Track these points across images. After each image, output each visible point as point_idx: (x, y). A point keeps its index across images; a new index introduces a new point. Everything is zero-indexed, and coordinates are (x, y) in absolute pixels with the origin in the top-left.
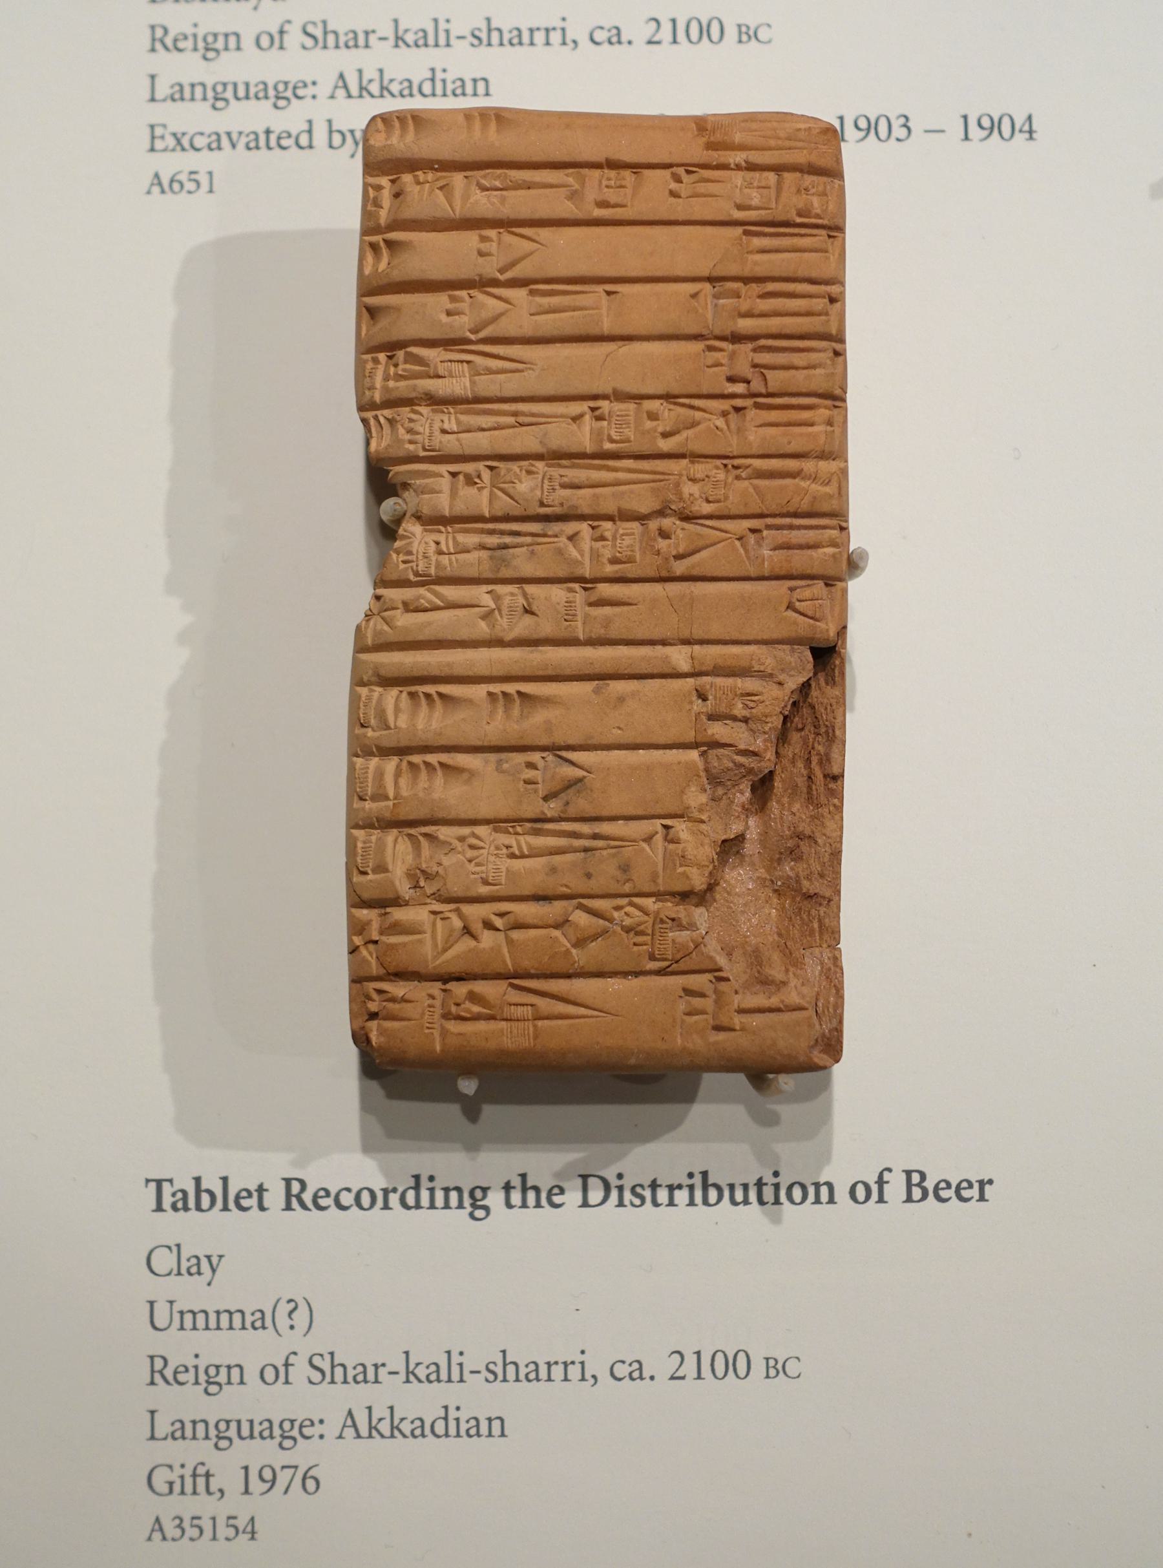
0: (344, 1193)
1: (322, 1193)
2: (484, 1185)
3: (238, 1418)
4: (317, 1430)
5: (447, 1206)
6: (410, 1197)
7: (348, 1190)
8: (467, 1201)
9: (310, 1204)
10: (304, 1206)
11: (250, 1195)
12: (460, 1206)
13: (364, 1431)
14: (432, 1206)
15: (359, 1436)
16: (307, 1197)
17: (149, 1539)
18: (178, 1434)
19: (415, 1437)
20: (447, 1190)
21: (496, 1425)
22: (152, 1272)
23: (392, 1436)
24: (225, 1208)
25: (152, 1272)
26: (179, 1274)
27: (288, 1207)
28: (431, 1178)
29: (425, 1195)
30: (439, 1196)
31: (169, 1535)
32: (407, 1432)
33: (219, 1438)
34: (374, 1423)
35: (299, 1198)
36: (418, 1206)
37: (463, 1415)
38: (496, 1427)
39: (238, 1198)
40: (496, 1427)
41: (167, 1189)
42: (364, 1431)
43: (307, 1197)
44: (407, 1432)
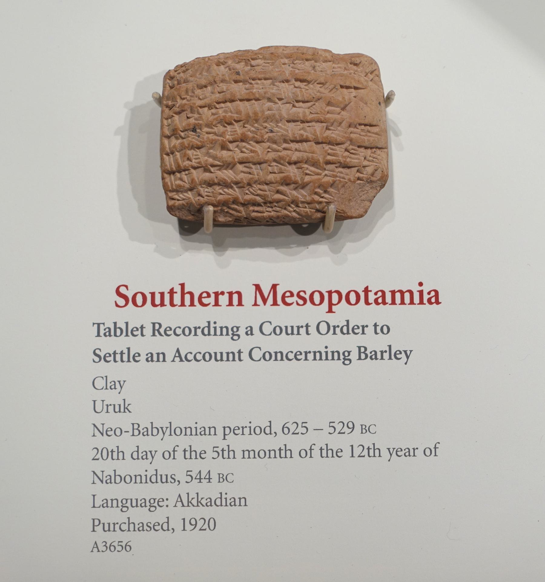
13: (186, 504)
23: (198, 506)
42: (186, 504)
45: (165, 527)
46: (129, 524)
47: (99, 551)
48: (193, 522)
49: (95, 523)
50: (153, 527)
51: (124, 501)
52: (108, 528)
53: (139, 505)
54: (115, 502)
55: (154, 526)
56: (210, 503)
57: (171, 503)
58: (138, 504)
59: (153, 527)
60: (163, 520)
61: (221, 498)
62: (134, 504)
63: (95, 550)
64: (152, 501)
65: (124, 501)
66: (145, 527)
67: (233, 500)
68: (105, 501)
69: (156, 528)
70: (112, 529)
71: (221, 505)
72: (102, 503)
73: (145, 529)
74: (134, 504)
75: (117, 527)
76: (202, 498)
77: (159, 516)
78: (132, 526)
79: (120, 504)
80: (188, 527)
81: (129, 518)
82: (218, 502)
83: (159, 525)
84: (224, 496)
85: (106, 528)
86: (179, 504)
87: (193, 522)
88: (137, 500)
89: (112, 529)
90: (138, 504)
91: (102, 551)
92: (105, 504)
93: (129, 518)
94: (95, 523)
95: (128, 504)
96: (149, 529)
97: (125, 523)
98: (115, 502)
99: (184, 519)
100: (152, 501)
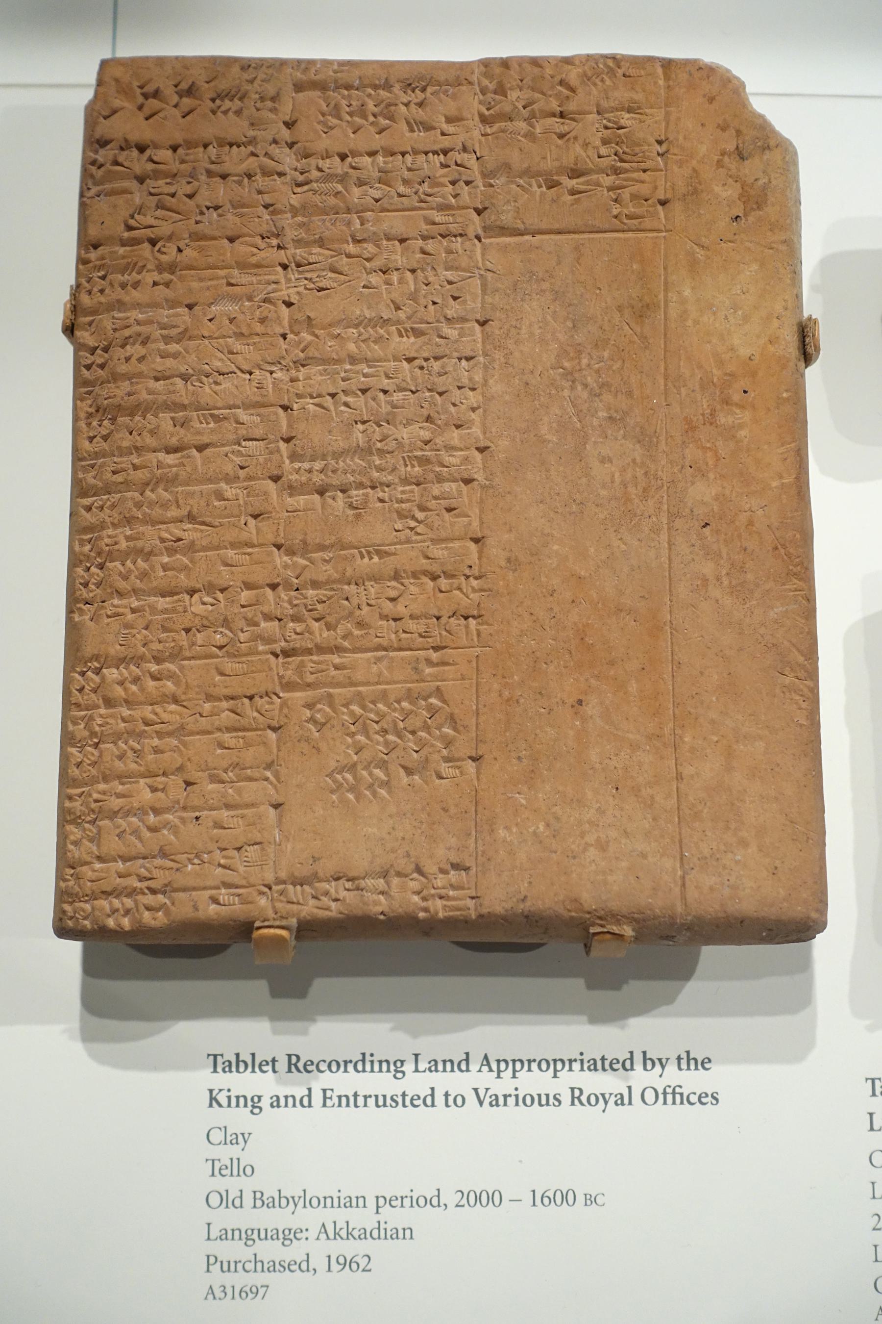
0: (322, 1063)
1: (309, 1063)
2: (402, 1059)
3: (258, 1227)
4: (304, 1235)
5: (381, 1071)
6: (360, 1067)
7: (324, 1061)
8: (392, 1068)
9: (302, 1069)
10: (298, 1070)
11: (267, 1064)
12: (388, 1071)
13: (331, 1236)
14: (372, 1071)
15: (328, 1238)
16: (300, 1065)
17: (206, 1298)
18: (224, 1237)
19: (360, 1239)
20: (380, 1062)
21: (408, 1232)
22: (209, 1142)
23: (348, 1238)
24: (253, 1071)
25: (209, 1142)
26: (225, 1144)
27: (290, 1071)
28: (372, 1055)
29: (368, 1067)
30: (376, 1067)
31: (217, 1296)
32: (357, 1236)
33: (247, 1239)
34: (337, 1231)
35: (295, 1065)
36: (364, 1071)
37: (389, 1227)
38: (407, 1233)
39: (260, 1065)
40: (407, 1233)
41: (220, 1060)
42: (331, 1236)
43: (300, 1065)
44: (357, 1236)
45: (304, 1266)
46: (256, 1263)
47: (214, 1298)
49: (210, 1261)
50: (287, 1267)
51: (249, 1232)
52: (228, 1267)
53: (269, 1237)
54: (237, 1233)
55: (289, 1265)
56: (365, 1235)
57: (313, 1233)
58: (266, 1235)
59: (287, 1267)
60: (300, 1257)
61: (379, 1228)
62: (263, 1235)
63: (210, 1297)
64: (287, 1232)
65: (249, 1232)
66: (277, 1267)
67: (394, 1231)
68: (224, 1232)
69: (292, 1268)
71: (379, 1238)
72: (219, 1234)
73: (277, 1269)
74: (263, 1235)
75: (240, 1266)
76: (353, 1229)
77: (295, 1252)
78: (259, 1265)
79: (244, 1236)
80: (335, 1267)
81: (255, 1255)
82: (375, 1234)
83: (296, 1263)
84: (383, 1226)
85: (225, 1268)
86: (323, 1236)
87: (342, 1260)
88: (266, 1230)
90: (266, 1235)
91: (220, 1299)
92: (224, 1235)
93: (255, 1255)
94: (210, 1261)
95: (255, 1236)
96: (282, 1269)
97: (250, 1261)
98: (237, 1233)
99: (329, 1257)
100: (287, 1232)
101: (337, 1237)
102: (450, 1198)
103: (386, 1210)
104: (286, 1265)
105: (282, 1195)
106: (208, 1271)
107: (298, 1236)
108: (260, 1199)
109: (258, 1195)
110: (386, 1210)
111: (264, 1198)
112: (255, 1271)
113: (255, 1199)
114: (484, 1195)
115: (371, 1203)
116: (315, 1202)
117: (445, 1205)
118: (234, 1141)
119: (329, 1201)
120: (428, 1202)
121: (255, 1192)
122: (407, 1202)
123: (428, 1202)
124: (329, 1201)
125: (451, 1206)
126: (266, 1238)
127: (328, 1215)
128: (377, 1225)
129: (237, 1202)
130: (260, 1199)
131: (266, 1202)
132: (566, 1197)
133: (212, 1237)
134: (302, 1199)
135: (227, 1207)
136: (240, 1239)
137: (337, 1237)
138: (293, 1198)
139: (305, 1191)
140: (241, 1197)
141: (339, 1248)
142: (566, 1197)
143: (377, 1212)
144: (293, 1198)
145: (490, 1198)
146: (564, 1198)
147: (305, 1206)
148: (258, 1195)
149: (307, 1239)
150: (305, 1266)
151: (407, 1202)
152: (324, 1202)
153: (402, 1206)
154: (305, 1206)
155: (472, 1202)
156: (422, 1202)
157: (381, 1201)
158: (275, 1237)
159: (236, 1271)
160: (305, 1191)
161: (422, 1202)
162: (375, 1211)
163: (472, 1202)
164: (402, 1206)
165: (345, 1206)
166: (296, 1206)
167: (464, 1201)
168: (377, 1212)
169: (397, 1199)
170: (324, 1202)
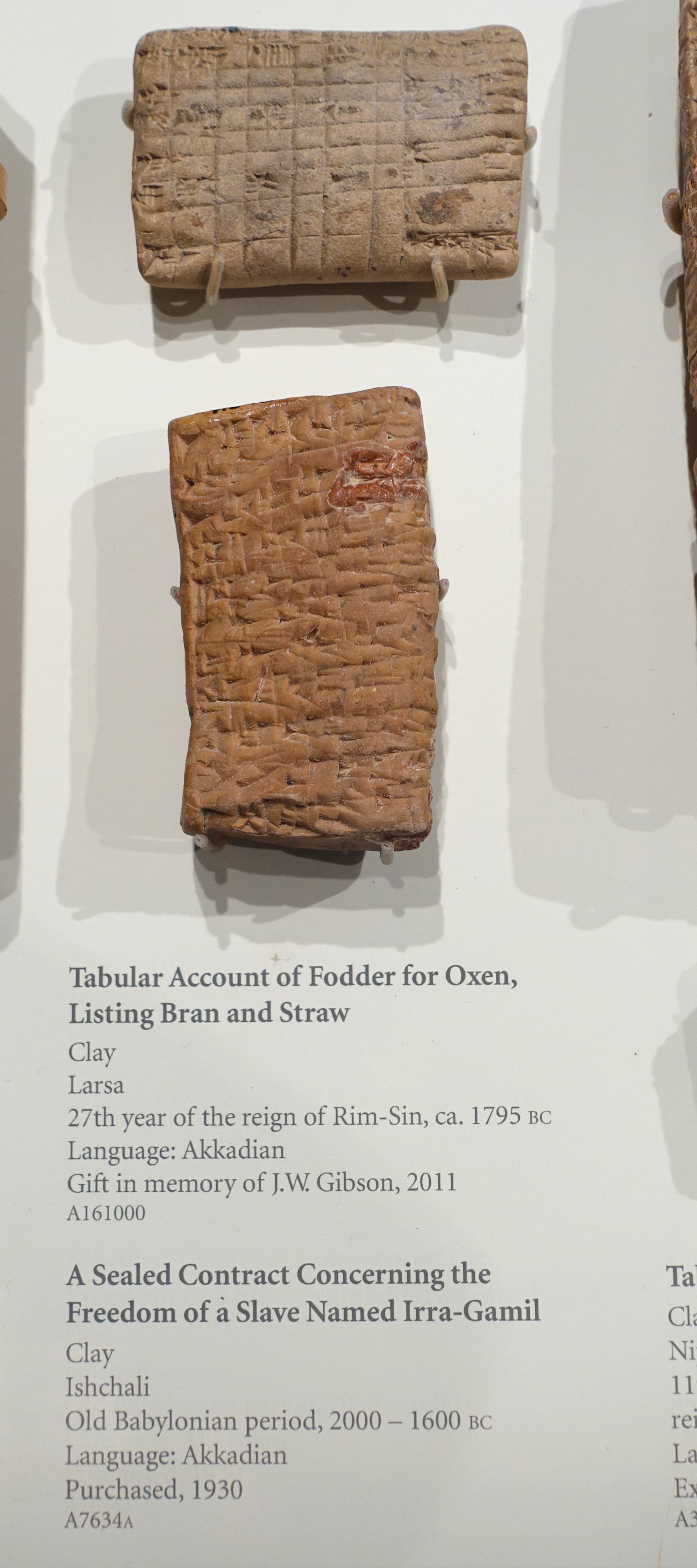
15: (196, 1462)
32: (226, 1460)
34: (205, 1454)
38: (279, 1457)
40: (279, 1457)
44: (226, 1460)
45: (170, 1492)
48: (210, 1486)
49: (71, 1486)
50: (152, 1493)
52: (89, 1494)
55: (154, 1491)
56: (234, 1459)
59: (152, 1493)
67: (266, 1455)
70: (94, 1494)
73: (141, 1495)
75: (102, 1492)
77: (161, 1477)
78: (123, 1491)
83: (161, 1489)
87: (210, 1486)
89: (94, 1494)
94: (71, 1486)
97: (113, 1487)
99: (197, 1482)
101: (205, 1461)
102: (325, 1419)
103: (257, 1432)
104: (151, 1491)
105: (147, 1416)
106: (69, 1497)
107: (164, 1459)
108: (124, 1420)
109: (122, 1416)
110: (257, 1432)
111: (128, 1419)
112: (119, 1497)
113: (118, 1420)
114: (362, 1417)
115: (241, 1425)
116: (181, 1424)
117: (320, 1427)
118: (96, 1358)
119: (196, 1422)
120: (302, 1423)
121: (118, 1413)
122: (279, 1424)
123: (302, 1423)
124: (196, 1422)
125: (327, 1428)
126: (130, 1462)
127: (195, 1438)
128: (247, 1449)
129: (99, 1424)
130: (124, 1420)
131: (130, 1423)
132: (449, 1420)
133: (72, 1461)
134: (168, 1420)
135: (88, 1428)
136: (103, 1462)
137: (205, 1461)
138: (158, 1419)
139: (171, 1411)
140: (103, 1418)
141: (205, 1473)
142: (449, 1420)
143: (248, 1435)
144: (158, 1419)
145: (369, 1421)
146: (448, 1420)
147: (171, 1428)
148: (122, 1416)
149: (173, 1463)
150: (171, 1492)
151: (279, 1424)
152: (191, 1423)
153: (274, 1428)
154: (171, 1428)
155: (349, 1424)
156: (295, 1423)
157: (252, 1423)
158: (139, 1460)
159: (98, 1497)
160: (171, 1411)
161: (295, 1423)
162: (245, 1433)
163: (349, 1424)
164: (274, 1428)
165: (214, 1428)
166: (161, 1427)
167: (340, 1423)
168: (248, 1435)
169: (269, 1420)
170: (191, 1423)
